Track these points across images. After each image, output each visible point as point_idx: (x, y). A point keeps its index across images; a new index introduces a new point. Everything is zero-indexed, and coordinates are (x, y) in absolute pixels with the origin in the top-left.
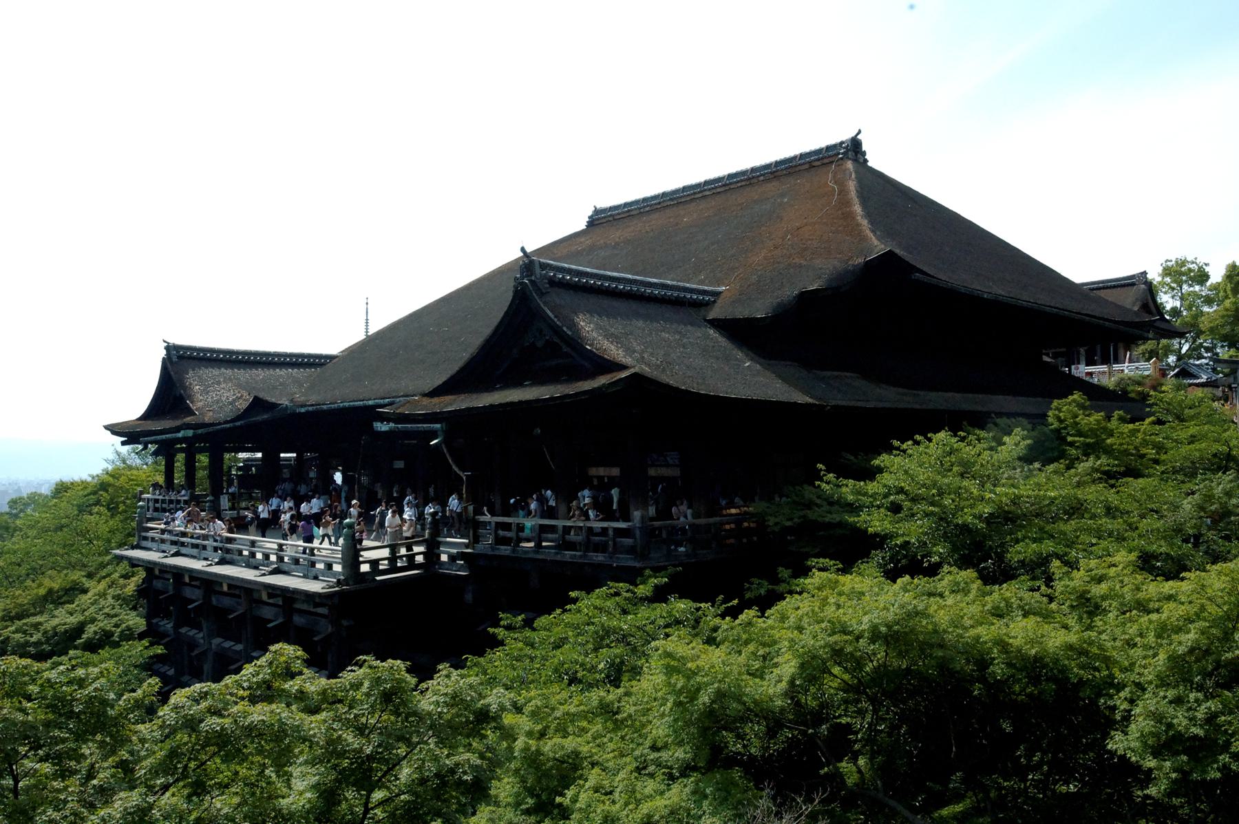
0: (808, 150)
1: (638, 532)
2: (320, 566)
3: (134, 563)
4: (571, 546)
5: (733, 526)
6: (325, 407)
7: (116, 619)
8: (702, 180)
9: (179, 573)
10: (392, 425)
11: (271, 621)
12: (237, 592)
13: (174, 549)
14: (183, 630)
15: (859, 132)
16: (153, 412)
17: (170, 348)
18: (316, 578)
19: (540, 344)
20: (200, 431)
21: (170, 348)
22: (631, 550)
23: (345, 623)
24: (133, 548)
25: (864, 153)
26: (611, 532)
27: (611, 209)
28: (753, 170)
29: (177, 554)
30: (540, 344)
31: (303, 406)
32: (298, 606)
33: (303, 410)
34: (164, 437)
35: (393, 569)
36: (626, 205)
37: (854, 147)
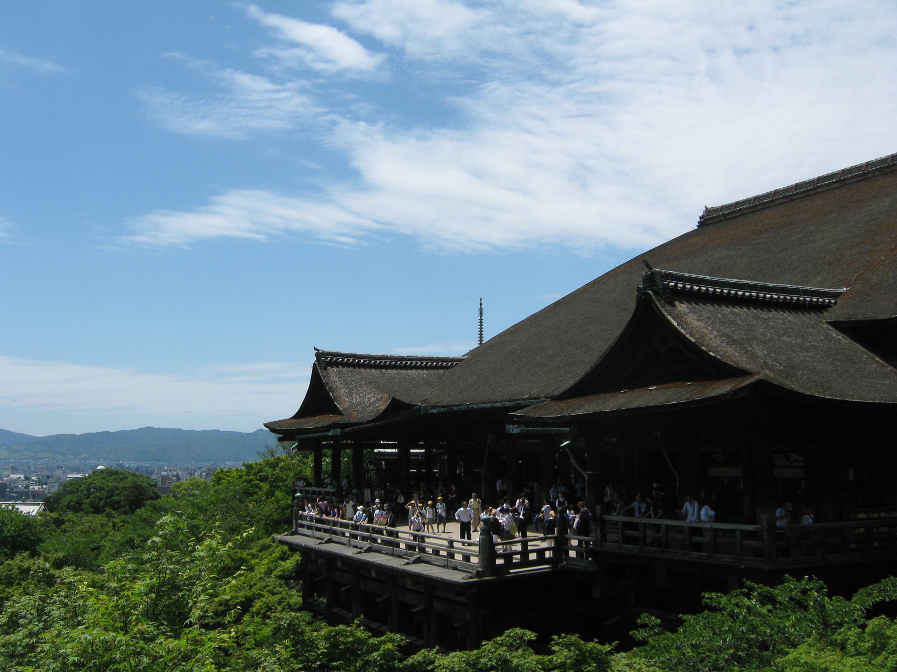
2: (458, 557)
3: (294, 548)
4: (698, 547)
7: (279, 596)
9: (331, 558)
10: (523, 428)
11: (414, 607)
13: (327, 536)
14: (335, 610)
16: (306, 410)
18: (455, 568)
21: (319, 355)
24: (293, 534)
26: (738, 534)
27: (722, 208)
28: (868, 164)
29: (330, 541)
31: (434, 407)
33: (435, 411)
35: (525, 562)
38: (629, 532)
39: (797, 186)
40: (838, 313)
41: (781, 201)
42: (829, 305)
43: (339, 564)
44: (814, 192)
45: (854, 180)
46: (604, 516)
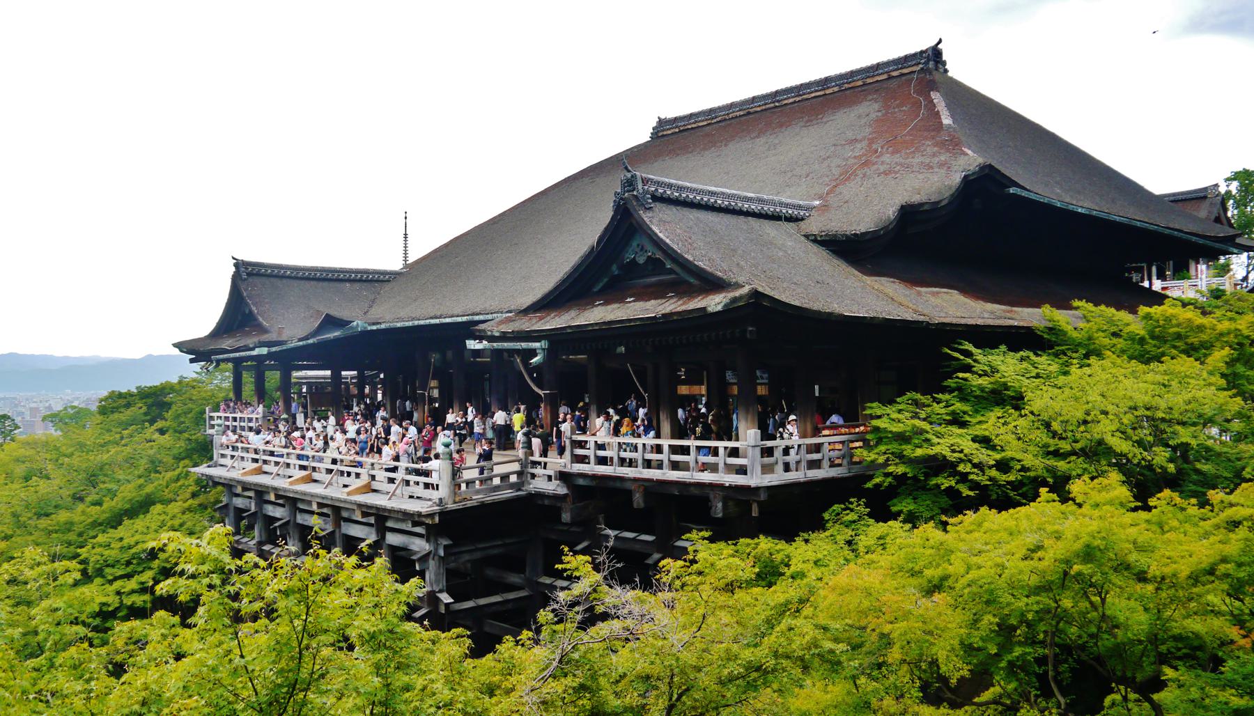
0: (885, 59)
1: (750, 451)
4: (675, 466)
6: (399, 325)
8: (774, 90)
11: (364, 540)
12: (325, 510)
15: (940, 41)
17: (240, 265)
18: (411, 497)
19: (641, 260)
20: (274, 349)
21: (240, 265)
22: (742, 470)
23: (445, 542)
25: (944, 63)
26: (721, 451)
29: (260, 471)
30: (641, 260)
32: (390, 524)
33: (374, 328)
34: (237, 355)
36: (691, 115)
37: (935, 55)
38: (601, 453)
43: (272, 498)
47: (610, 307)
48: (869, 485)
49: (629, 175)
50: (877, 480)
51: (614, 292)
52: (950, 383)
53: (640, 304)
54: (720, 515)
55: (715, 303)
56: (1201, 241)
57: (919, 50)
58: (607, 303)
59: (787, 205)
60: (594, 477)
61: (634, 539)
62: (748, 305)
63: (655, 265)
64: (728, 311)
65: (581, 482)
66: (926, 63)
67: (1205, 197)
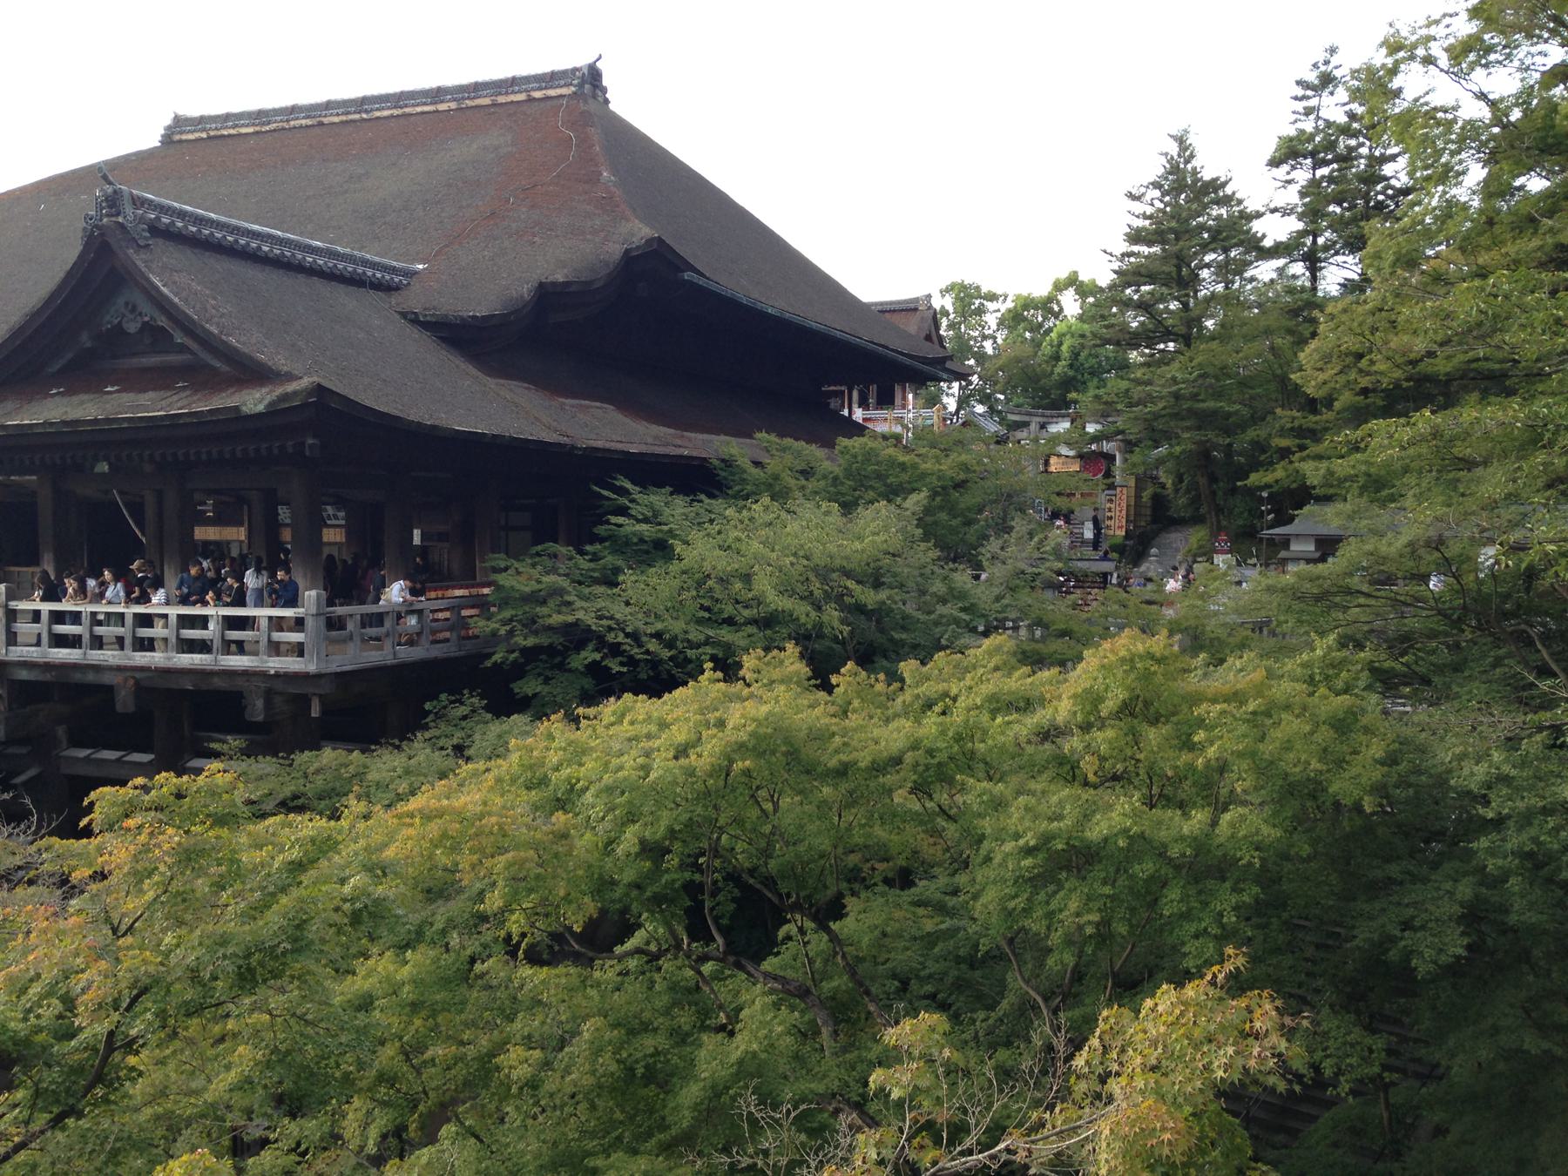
0: (525, 73)
5: (447, 614)
19: (132, 327)
22: (299, 650)
25: (604, 90)
30: (132, 327)
39: (328, 105)
40: (414, 300)
41: (304, 122)
42: (397, 288)
44: (357, 116)
45: (419, 109)
46: (13, 604)
47: (75, 399)
48: (488, 664)
49: (109, 189)
50: (497, 657)
51: (83, 374)
52: (601, 530)
53: (128, 398)
54: (260, 718)
55: (254, 401)
56: (908, 361)
57: (569, 66)
58: (70, 392)
59: (374, 265)
60: (48, 667)
61: (119, 760)
62: (304, 406)
63: (156, 337)
64: (272, 413)
65: (24, 675)
66: (581, 86)
67: (916, 309)
